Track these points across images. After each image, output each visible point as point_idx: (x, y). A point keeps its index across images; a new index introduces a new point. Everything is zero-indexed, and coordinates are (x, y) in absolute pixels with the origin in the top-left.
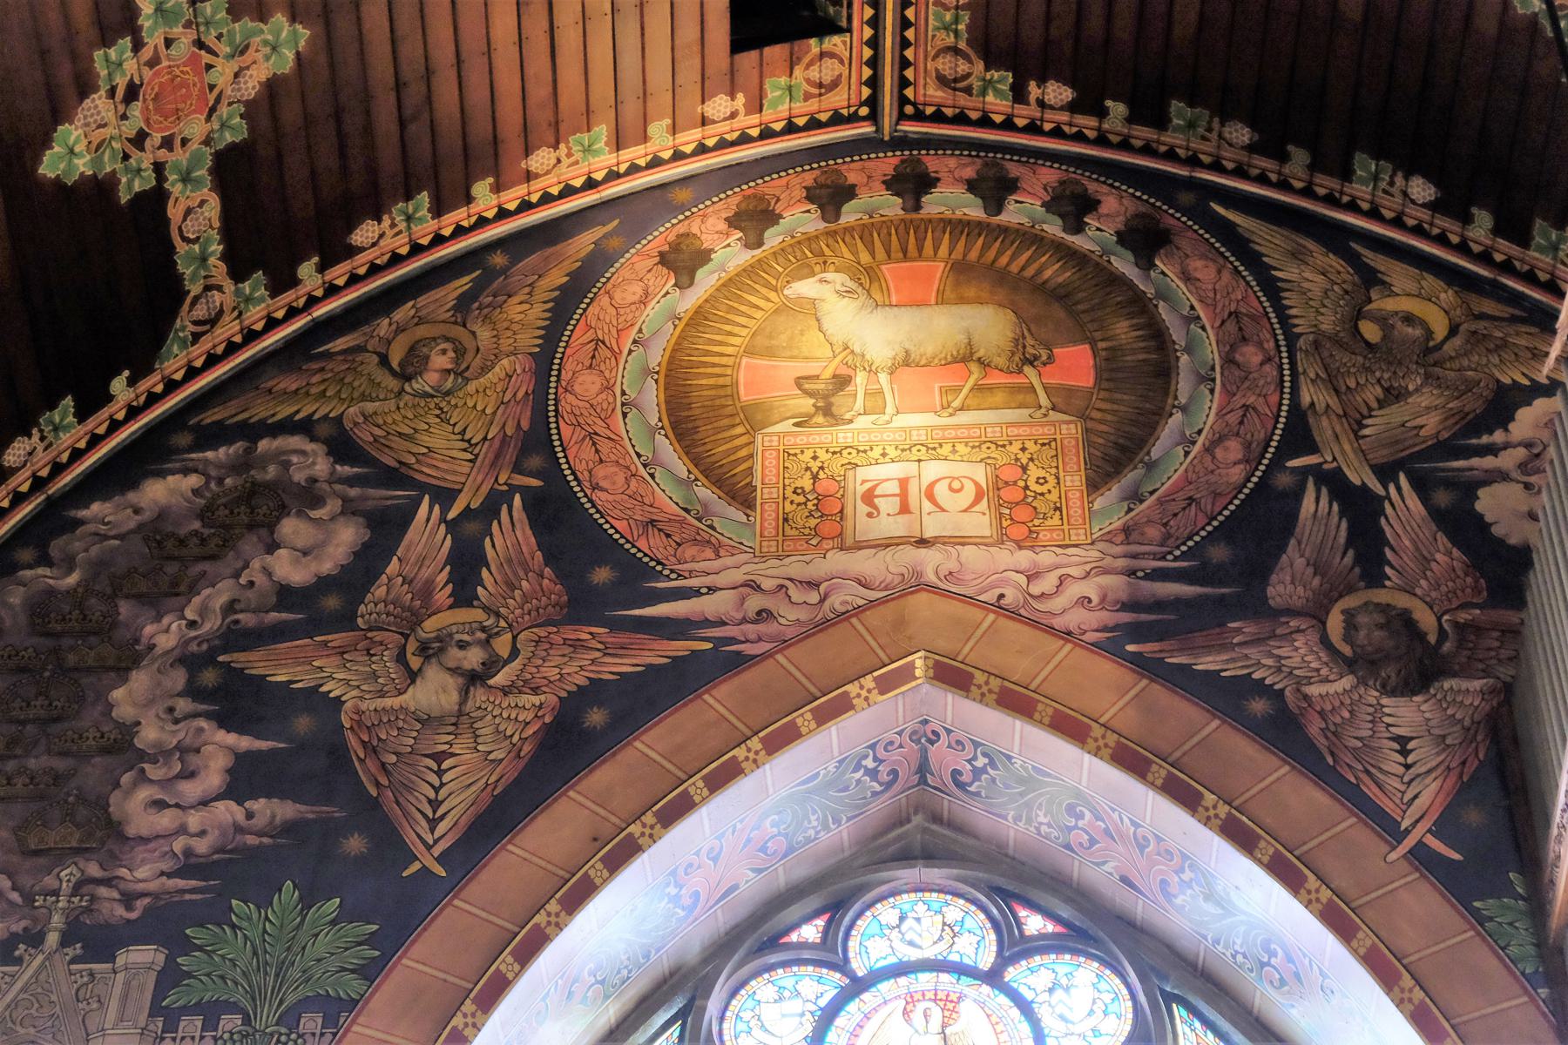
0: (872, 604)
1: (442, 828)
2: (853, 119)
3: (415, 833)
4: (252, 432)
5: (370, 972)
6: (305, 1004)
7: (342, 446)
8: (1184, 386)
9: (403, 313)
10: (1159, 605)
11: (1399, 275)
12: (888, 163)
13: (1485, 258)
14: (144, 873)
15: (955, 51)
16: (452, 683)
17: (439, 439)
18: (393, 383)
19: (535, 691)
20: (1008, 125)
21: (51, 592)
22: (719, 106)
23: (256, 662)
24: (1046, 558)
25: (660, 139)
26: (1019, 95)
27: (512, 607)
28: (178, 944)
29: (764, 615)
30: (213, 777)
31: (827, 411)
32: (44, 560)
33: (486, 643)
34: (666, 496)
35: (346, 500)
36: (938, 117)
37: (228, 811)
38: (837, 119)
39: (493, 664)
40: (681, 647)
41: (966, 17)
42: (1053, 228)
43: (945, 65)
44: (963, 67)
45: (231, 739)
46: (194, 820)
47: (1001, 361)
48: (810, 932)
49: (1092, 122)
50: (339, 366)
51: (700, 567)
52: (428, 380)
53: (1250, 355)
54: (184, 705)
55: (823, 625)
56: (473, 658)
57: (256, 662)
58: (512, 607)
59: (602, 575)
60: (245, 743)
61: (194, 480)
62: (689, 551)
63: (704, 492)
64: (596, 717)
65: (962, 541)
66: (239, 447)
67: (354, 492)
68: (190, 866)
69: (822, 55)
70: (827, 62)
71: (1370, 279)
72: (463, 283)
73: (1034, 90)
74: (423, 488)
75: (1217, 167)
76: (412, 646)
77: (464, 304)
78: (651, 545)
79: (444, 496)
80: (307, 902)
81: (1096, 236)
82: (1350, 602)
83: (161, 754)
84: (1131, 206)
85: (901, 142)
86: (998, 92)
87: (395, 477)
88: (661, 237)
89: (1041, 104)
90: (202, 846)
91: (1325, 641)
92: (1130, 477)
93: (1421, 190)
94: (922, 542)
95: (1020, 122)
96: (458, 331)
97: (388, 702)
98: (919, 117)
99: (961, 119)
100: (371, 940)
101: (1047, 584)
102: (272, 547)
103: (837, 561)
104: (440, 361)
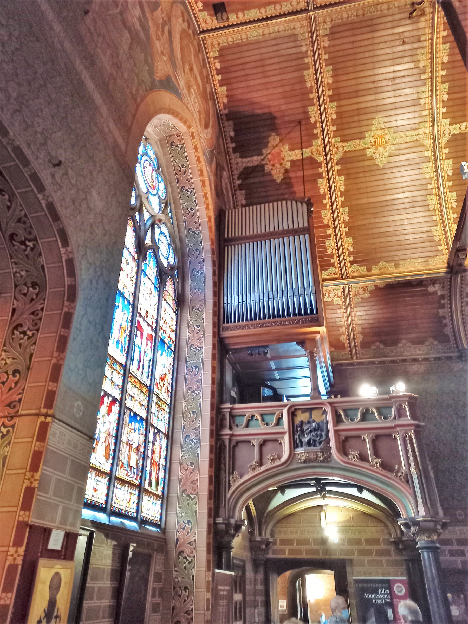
2: (199, 28)
15: (219, 44)
26: (215, 58)
38: (199, 26)
41: (227, 44)
43: (215, 43)
44: (216, 46)
49: (215, 73)
69: (212, 21)
70: (211, 21)
73: (217, 61)
86: (213, 54)
89: (215, 63)
95: (209, 60)
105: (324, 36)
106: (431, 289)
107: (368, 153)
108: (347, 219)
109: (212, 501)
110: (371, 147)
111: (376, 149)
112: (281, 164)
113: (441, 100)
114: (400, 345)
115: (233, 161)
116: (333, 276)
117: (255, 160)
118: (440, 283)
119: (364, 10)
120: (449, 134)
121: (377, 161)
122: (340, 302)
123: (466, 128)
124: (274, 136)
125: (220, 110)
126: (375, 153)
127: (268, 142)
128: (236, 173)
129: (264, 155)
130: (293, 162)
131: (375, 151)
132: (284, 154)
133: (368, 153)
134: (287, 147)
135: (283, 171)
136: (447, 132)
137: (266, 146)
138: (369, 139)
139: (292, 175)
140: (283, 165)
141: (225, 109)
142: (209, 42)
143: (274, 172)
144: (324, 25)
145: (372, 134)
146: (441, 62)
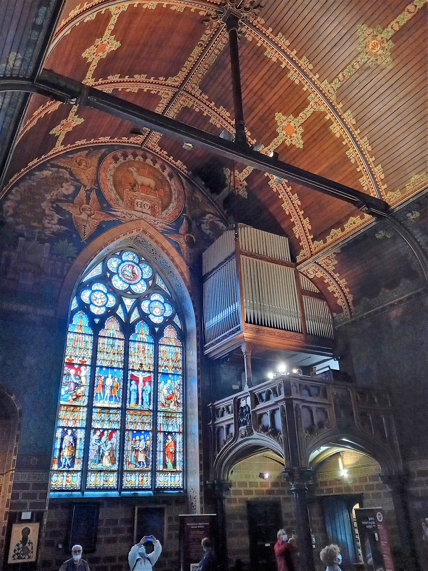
0: (137, 220)
1: (85, 236)
3: (82, 236)
4: (59, 167)
5: (78, 254)
6: (69, 257)
7: (71, 174)
8: (173, 199)
9: (79, 154)
10: (168, 229)
11: (197, 192)
12: (142, 152)
13: (207, 194)
14: (47, 233)
16: (86, 216)
17: (84, 177)
18: (78, 165)
19: (97, 220)
20: (157, 153)
21: (32, 185)
22: (125, 138)
23: (60, 204)
24: (156, 219)
25: (116, 139)
26: (161, 150)
27: (94, 206)
28: (52, 244)
29: (124, 217)
30: (55, 221)
31: (133, 189)
32: (30, 179)
33: (90, 211)
34: (113, 195)
35: (72, 183)
36: (149, 148)
37: (58, 226)
39: (91, 215)
40: (114, 219)
42: (161, 170)
43: (153, 143)
45: (58, 215)
46: (54, 227)
47: (153, 188)
48: (118, 253)
50: (70, 159)
51: (117, 208)
52: (82, 167)
53: (180, 197)
54: (51, 209)
55: (131, 221)
56: (89, 213)
57: (60, 204)
58: (94, 206)
59: (105, 205)
60: (60, 217)
61: (50, 173)
62: (116, 205)
63: (118, 197)
64: (104, 226)
65: (147, 214)
66: (56, 169)
67: (73, 182)
68: (53, 233)
71: (194, 191)
72: (87, 152)
74: (83, 184)
75: (180, 169)
76: (81, 209)
77: (87, 155)
78: (111, 202)
79: (85, 186)
80: (69, 243)
81: (165, 174)
82: (188, 235)
83: (48, 215)
84: (170, 171)
85: (143, 150)
87: (78, 181)
88: (112, 153)
90: (55, 231)
91: (184, 239)
92: (166, 210)
93: (203, 183)
94: (143, 212)
96: (86, 159)
97: (78, 216)
98: (147, 147)
99: (152, 150)
100: (77, 250)
101: (156, 223)
102: (62, 187)
103: (133, 212)
104: (84, 164)
105: (201, 95)
106: (378, 236)
107: (287, 143)
108: (299, 203)
109: (202, 471)
110: (286, 138)
111: (291, 137)
112: (241, 185)
113: (309, 71)
114: (381, 294)
115: (215, 199)
116: (304, 258)
117: (225, 192)
118: (381, 230)
119: (207, 64)
120: (334, 90)
121: (297, 147)
122: (321, 275)
123: (344, 77)
124: (225, 169)
125: (187, 174)
126: (292, 141)
127: (225, 175)
128: (221, 205)
129: (228, 185)
130: (247, 179)
131: (291, 139)
132: (237, 179)
133: (288, 143)
134: (237, 172)
135: (244, 189)
136: (332, 91)
137: (225, 179)
138: (282, 134)
139: (252, 188)
140: (243, 185)
141: (189, 172)
142: (150, 145)
143: (240, 193)
144: (194, 90)
145: (281, 128)
146: (286, 47)
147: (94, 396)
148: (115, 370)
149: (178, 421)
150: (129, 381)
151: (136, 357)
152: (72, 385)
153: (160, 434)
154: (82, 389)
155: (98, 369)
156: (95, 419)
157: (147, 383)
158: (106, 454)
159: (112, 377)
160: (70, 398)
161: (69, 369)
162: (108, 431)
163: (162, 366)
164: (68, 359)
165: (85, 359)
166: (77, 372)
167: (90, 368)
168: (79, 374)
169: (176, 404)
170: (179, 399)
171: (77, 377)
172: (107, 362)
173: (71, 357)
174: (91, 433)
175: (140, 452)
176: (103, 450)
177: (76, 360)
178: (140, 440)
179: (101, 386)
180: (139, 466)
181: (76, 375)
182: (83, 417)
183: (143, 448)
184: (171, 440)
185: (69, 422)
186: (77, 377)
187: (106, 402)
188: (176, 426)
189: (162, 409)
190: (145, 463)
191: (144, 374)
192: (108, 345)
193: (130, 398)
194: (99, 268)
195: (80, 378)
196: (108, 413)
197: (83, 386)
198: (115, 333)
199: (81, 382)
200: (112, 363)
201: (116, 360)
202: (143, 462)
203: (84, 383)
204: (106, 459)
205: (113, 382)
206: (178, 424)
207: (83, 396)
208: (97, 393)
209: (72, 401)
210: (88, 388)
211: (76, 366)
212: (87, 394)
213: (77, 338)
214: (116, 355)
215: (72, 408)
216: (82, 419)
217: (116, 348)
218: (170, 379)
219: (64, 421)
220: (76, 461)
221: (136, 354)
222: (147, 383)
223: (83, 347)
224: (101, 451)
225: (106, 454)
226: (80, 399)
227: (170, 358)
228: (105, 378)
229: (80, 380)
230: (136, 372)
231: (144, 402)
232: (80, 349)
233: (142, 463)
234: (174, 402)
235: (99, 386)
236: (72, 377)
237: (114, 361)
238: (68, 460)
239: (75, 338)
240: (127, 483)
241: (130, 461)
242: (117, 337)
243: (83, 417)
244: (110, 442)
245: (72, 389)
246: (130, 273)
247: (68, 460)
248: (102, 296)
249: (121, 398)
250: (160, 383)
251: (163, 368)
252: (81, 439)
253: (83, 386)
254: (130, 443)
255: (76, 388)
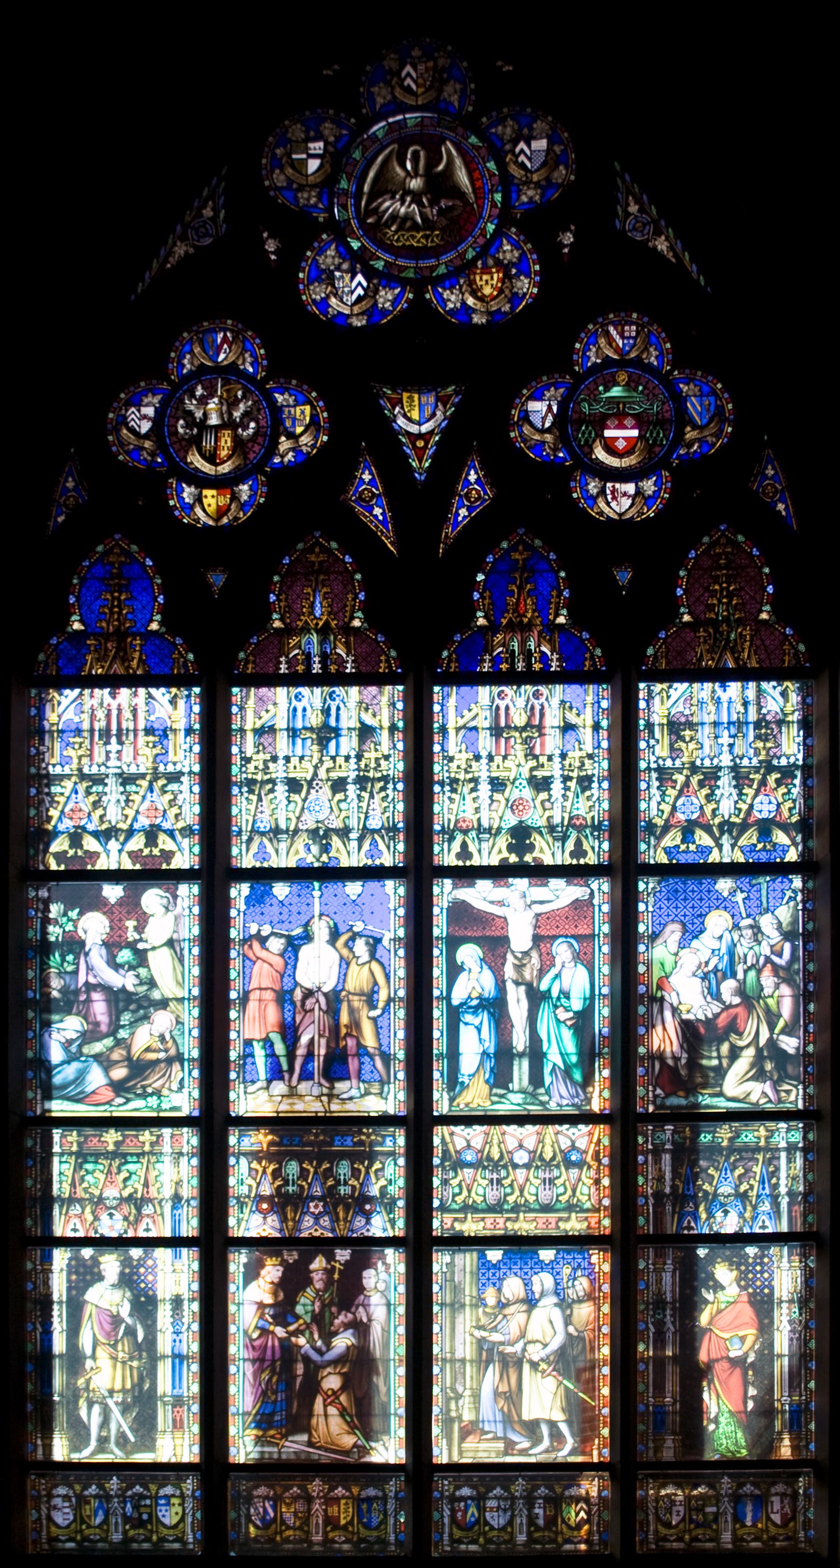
147: (233, 1055)
148: (353, 888)
149: (783, 1174)
150: (438, 952)
151: (484, 788)
152: (99, 1008)
153: (660, 1255)
154: (162, 1020)
155: (240, 892)
156: (244, 1190)
157: (562, 951)
158: (332, 1382)
159: (334, 935)
160: (96, 1078)
161: (73, 914)
162: (330, 1257)
163: (666, 828)
164: (60, 857)
165: (165, 843)
166: (117, 927)
167: (196, 889)
168: (132, 935)
169: (769, 1066)
170: (788, 1030)
171: (125, 956)
172: (301, 841)
173: (76, 839)
174: (232, 1267)
175: (534, 1365)
176: (307, 1359)
177: (114, 854)
178: (530, 1302)
179: (269, 995)
180: (526, 1444)
181: (112, 945)
182: (178, 1183)
183: (556, 1343)
184: (732, 1291)
185: (104, 1217)
186: (125, 956)
187: (303, 1087)
188: (766, 1207)
189: (674, 1101)
190: (564, 1428)
191: (538, 892)
192: (293, 733)
193: (453, 1055)
194: (208, 212)
195: (141, 958)
196: (320, 1157)
197: (163, 1004)
198: (342, 651)
199: (152, 983)
200: (326, 849)
201: (353, 823)
202: (552, 1424)
203: (167, 987)
204: (332, 1410)
205: (345, 963)
206: (783, 1190)
207: (169, 1061)
208: (248, 1043)
209: (109, 1094)
210: (196, 1012)
211: (113, 892)
212: (191, 1049)
213: (100, 714)
214: (352, 790)
215: (111, 1137)
216: (177, 1199)
217: (348, 744)
218: (724, 904)
219: (76, 1209)
220: (163, 1416)
221: (481, 770)
222: (562, 951)
223: (145, 765)
224: (300, 1369)
225: (332, 1382)
226: (154, 1081)
227: (726, 760)
228: (293, 946)
229: (143, 971)
230: (484, 886)
231: (547, 1069)
232: (126, 780)
233: (545, 1430)
234: (750, 1052)
235: (254, 996)
236: (97, 957)
237: (344, 833)
238: (116, 1413)
239: (93, 717)
240: (458, 1533)
241: (468, 1416)
242: (349, 669)
243: (178, 1183)
244: (343, 1318)
245: (104, 1028)
246: (416, 197)
247: (116, 1413)
248: (233, 404)
249: (401, 1055)
250: (654, 937)
251: (672, 839)
252: (177, 1302)
253: (163, 1004)
254: (466, 1320)
255: (126, 1018)
